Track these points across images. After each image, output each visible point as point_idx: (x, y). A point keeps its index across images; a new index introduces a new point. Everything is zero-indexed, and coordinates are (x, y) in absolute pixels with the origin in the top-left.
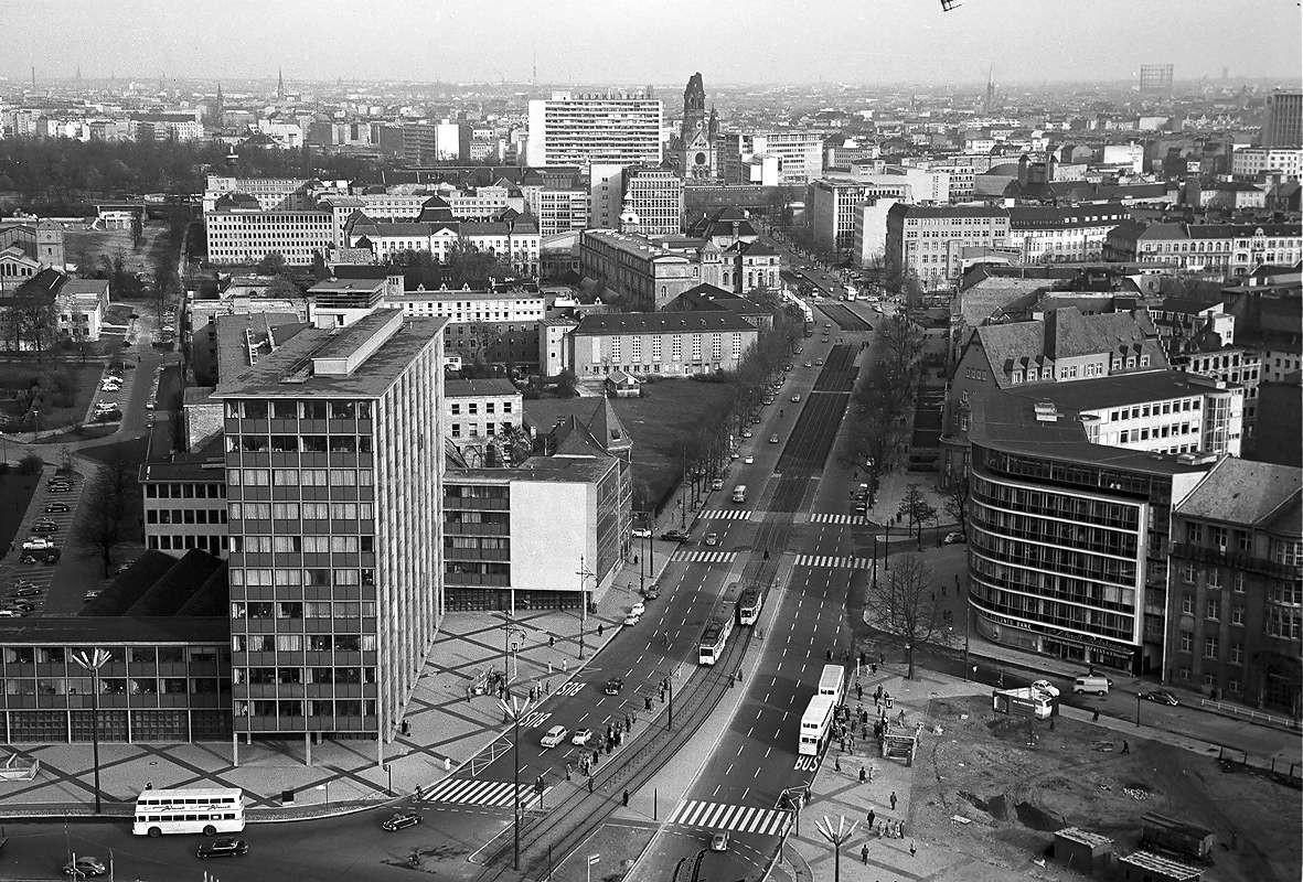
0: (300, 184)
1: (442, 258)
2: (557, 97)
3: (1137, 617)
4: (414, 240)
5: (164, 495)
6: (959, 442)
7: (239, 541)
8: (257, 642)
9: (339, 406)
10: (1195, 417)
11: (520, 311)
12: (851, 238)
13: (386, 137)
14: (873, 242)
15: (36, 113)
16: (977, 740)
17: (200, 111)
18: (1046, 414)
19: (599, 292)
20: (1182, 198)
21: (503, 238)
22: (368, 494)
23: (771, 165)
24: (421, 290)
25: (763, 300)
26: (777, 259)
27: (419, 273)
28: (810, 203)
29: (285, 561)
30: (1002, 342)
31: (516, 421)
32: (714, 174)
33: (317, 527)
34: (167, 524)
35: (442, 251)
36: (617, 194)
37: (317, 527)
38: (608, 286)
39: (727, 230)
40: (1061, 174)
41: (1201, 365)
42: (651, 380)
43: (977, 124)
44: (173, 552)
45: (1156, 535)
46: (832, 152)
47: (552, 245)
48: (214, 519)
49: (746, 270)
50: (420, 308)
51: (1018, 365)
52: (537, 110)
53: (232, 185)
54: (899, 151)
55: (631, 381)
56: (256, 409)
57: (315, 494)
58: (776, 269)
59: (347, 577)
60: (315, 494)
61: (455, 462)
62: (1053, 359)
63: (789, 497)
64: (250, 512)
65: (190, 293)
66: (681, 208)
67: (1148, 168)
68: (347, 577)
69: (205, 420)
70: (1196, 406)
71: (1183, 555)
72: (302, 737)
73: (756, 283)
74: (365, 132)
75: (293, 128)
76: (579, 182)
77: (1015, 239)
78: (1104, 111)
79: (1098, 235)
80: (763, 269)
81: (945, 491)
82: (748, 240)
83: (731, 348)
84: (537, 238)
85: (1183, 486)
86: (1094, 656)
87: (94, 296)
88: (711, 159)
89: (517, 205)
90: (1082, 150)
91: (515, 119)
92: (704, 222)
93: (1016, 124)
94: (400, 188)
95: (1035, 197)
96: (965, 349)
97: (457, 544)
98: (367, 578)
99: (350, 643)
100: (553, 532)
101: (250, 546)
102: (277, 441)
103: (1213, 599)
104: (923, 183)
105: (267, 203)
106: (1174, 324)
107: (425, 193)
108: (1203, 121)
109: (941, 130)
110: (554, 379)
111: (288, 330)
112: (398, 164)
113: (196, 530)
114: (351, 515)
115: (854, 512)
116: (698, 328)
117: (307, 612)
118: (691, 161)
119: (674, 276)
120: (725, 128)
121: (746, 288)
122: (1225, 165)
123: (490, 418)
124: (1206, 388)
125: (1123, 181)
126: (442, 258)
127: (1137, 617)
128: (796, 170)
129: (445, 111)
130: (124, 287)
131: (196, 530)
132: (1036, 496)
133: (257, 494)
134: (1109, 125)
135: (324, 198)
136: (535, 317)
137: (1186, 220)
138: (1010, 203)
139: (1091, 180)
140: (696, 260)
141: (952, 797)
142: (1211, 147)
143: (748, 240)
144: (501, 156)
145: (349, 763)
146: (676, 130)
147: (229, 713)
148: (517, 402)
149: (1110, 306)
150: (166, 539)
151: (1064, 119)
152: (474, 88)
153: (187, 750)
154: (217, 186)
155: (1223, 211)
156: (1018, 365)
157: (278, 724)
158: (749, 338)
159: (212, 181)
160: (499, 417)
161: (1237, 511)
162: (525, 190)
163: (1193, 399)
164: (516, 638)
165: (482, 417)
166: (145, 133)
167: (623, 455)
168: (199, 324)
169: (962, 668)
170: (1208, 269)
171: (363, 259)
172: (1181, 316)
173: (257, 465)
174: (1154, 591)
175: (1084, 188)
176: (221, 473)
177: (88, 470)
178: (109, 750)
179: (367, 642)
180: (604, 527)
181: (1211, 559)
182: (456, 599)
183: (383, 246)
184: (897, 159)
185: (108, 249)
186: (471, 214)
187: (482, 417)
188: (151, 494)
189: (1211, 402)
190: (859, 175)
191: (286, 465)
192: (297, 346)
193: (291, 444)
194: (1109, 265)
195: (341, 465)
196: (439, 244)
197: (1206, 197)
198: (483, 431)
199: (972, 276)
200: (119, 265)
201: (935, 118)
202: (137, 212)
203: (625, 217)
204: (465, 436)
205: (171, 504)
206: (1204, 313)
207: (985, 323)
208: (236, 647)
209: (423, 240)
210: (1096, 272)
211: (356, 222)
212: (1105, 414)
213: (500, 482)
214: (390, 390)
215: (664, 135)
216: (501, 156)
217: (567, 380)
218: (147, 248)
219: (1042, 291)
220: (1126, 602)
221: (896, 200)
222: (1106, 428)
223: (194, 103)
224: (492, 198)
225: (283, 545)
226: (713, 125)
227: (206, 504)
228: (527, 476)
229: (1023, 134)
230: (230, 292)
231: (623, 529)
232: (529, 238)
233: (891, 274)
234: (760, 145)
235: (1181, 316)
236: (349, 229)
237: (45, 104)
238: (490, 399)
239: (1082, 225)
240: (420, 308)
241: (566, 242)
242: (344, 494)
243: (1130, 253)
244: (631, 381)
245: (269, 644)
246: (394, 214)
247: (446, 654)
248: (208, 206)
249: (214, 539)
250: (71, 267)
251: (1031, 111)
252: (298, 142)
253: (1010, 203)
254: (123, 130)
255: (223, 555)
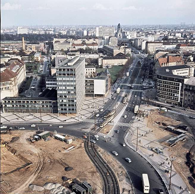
0: (66, 39)
1: (85, 49)
2: (100, 27)
3: (179, 98)
4: (81, 47)
5: (48, 81)
6: (155, 74)
7: (58, 87)
8: (61, 101)
9: (71, 69)
10: (188, 71)
11: (95, 56)
12: (140, 46)
13: (77, 33)
14: (143, 47)
15: (32, 30)
16: (157, 114)
17: (53, 30)
18: (167, 70)
19: (106, 54)
20: (186, 41)
21: (93, 46)
22: (75, 81)
23: (129, 36)
24: (82, 54)
25: (128, 55)
26: (130, 49)
27: (82, 51)
28: (135, 41)
29: (64, 90)
30: (161, 61)
31: (95, 71)
32: (122, 37)
33: (68, 86)
34: (49, 85)
35: (84, 48)
36: (109, 40)
37: (68, 86)
38: (107, 53)
39: (123, 45)
40: (170, 37)
41: (188, 64)
42: (113, 66)
43: (158, 30)
44: (50, 89)
45: (182, 87)
46: (138, 34)
47: (99, 47)
48: (55, 84)
49: (126, 51)
50: (82, 56)
51: (163, 64)
52: (97, 28)
53: (57, 40)
54: (147, 34)
55: (110, 66)
56: (60, 70)
57: (68, 81)
58: (130, 50)
59: (72, 92)
60: (68, 81)
61: (87, 77)
62: (168, 63)
63: (132, 82)
64: (60, 83)
65: (52, 54)
66: (117, 42)
67: (182, 37)
68: (72, 92)
69: (54, 71)
70: (188, 69)
71: (186, 90)
72: (67, 113)
73: (127, 52)
74: (74, 32)
75: (65, 32)
76: (103, 39)
77: (163, 46)
78: (176, 29)
79: (175, 46)
80: (129, 51)
81: (154, 81)
82: (126, 46)
83: (124, 61)
84: (97, 46)
85: (186, 81)
86: (173, 103)
87: (39, 55)
88: (121, 35)
89: (95, 42)
90: (173, 34)
91: (95, 30)
92: (120, 44)
93: (163, 30)
94: (79, 39)
95: (166, 40)
96: (156, 62)
97: (87, 88)
98: (75, 92)
99: (73, 101)
100: (100, 86)
101: (60, 88)
102: (63, 74)
103: (189, 95)
104: (151, 38)
105: (61, 42)
106: (185, 58)
107: (82, 40)
108: (189, 30)
109: (153, 31)
110: (100, 66)
111: (64, 59)
112: (79, 36)
113: (53, 86)
114: (73, 84)
115: (141, 84)
116: (119, 58)
117: (67, 97)
118: (118, 36)
119: (116, 52)
120: (123, 31)
121: (126, 53)
122: (192, 36)
123: (91, 71)
124: (189, 67)
125: (178, 38)
126: (85, 49)
127: (179, 98)
128: (133, 37)
129: (85, 29)
130: (43, 53)
131: (53, 86)
132: (166, 82)
133: (61, 81)
134: (176, 30)
135: (69, 41)
136: (97, 57)
137: (187, 44)
138: (163, 41)
139: (174, 38)
140: (119, 49)
141: (153, 122)
142: (190, 34)
143: (126, 46)
144: (93, 35)
145: (73, 117)
146: (116, 31)
147: (57, 110)
148: (95, 69)
149: (176, 56)
150: (49, 87)
151: (170, 30)
152: (89, 26)
153: (52, 115)
154: (55, 40)
155: (192, 43)
156: (163, 64)
157: (64, 111)
158: (127, 60)
159: (54, 39)
160: (92, 71)
161: (193, 84)
162: (96, 40)
163: (187, 69)
164: (95, 101)
165: (90, 71)
166: (46, 33)
167: (109, 76)
168: (53, 58)
169: (155, 105)
170: (190, 51)
171: (74, 49)
172: (186, 57)
173: (60, 77)
174: (181, 95)
175: (173, 39)
176: (56, 78)
177: (39, 78)
178: (43, 114)
179: (75, 101)
180: (107, 86)
181: (189, 90)
182: (87, 95)
183: (77, 48)
184: (147, 35)
185: (41, 48)
186: (90, 43)
187: (90, 71)
188: (47, 81)
189: (190, 69)
190: (142, 37)
191: (64, 77)
192: (66, 61)
193: (65, 74)
194: (176, 50)
195: (71, 77)
196: (84, 47)
197: (190, 41)
198: (90, 73)
199: (157, 51)
200: (42, 50)
201: (152, 29)
202: (45, 43)
203: (109, 43)
204: (88, 74)
205: (49, 82)
206: (189, 57)
207: (159, 58)
208: (58, 101)
209: (82, 47)
210: (175, 51)
211: (73, 44)
212: (175, 70)
213: (93, 80)
214: (78, 67)
215: (115, 32)
216: (93, 35)
217: (101, 67)
218: (46, 48)
219: (167, 53)
220: (178, 96)
221: (147, 41)
222: (175, 72)
223: (52, 29)
224: (91, 41)
225: (64, 88)
226: (121, 30)
227: (54, 82)
228: (96, 79)
229: (164, 32)
230: (57, 54)
231: (109, 86)
232: (96, 46)
233: (146, 51)
234: (128, 33)
235: (186, 57)
236: (72, 45)
237: (33, 29)
238: (91, 68)
239: (172, 44)
240: (82, 56)
241: (101, 47)
242: (72, 81)
243: (179, 48)
244: (110, 66)
245: (62, 101)
246: (78, 43)
247: (86, 103)
248: (54, 42)
249: (55, 87)
250: (36, 51)
251: (165, 29)
252: (65, 34)
253: (163, 41)
254: (42, 33)
255: (56, 89)
